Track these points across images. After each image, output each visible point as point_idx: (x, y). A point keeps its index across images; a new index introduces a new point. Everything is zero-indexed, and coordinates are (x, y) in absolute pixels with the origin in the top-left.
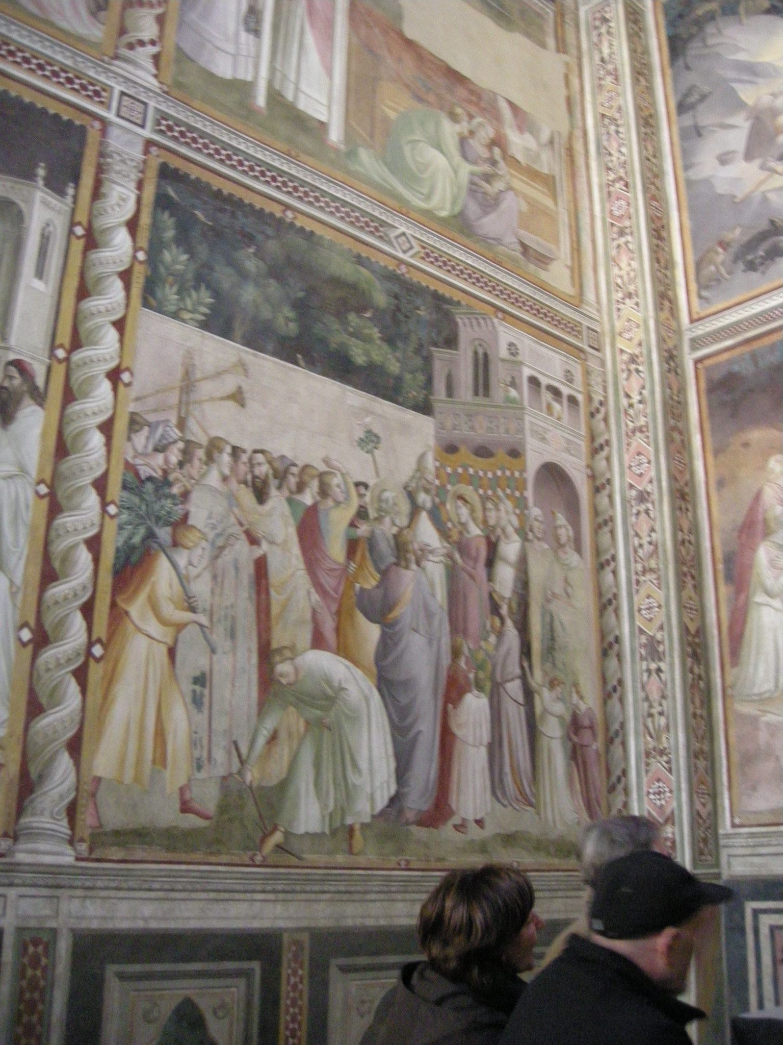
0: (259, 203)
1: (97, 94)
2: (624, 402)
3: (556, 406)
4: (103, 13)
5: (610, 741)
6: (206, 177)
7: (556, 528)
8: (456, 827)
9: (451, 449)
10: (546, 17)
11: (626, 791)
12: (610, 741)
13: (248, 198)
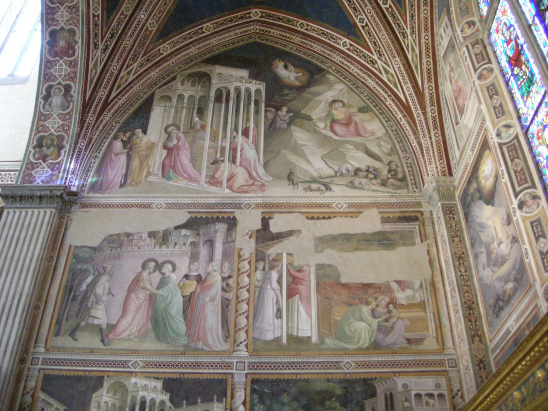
0: (286, 377)
1: (229, 366)
3: (431, 401)
4: (228, 339)
6: (266, 377)
10: (414, 230)
13: (282, 377)
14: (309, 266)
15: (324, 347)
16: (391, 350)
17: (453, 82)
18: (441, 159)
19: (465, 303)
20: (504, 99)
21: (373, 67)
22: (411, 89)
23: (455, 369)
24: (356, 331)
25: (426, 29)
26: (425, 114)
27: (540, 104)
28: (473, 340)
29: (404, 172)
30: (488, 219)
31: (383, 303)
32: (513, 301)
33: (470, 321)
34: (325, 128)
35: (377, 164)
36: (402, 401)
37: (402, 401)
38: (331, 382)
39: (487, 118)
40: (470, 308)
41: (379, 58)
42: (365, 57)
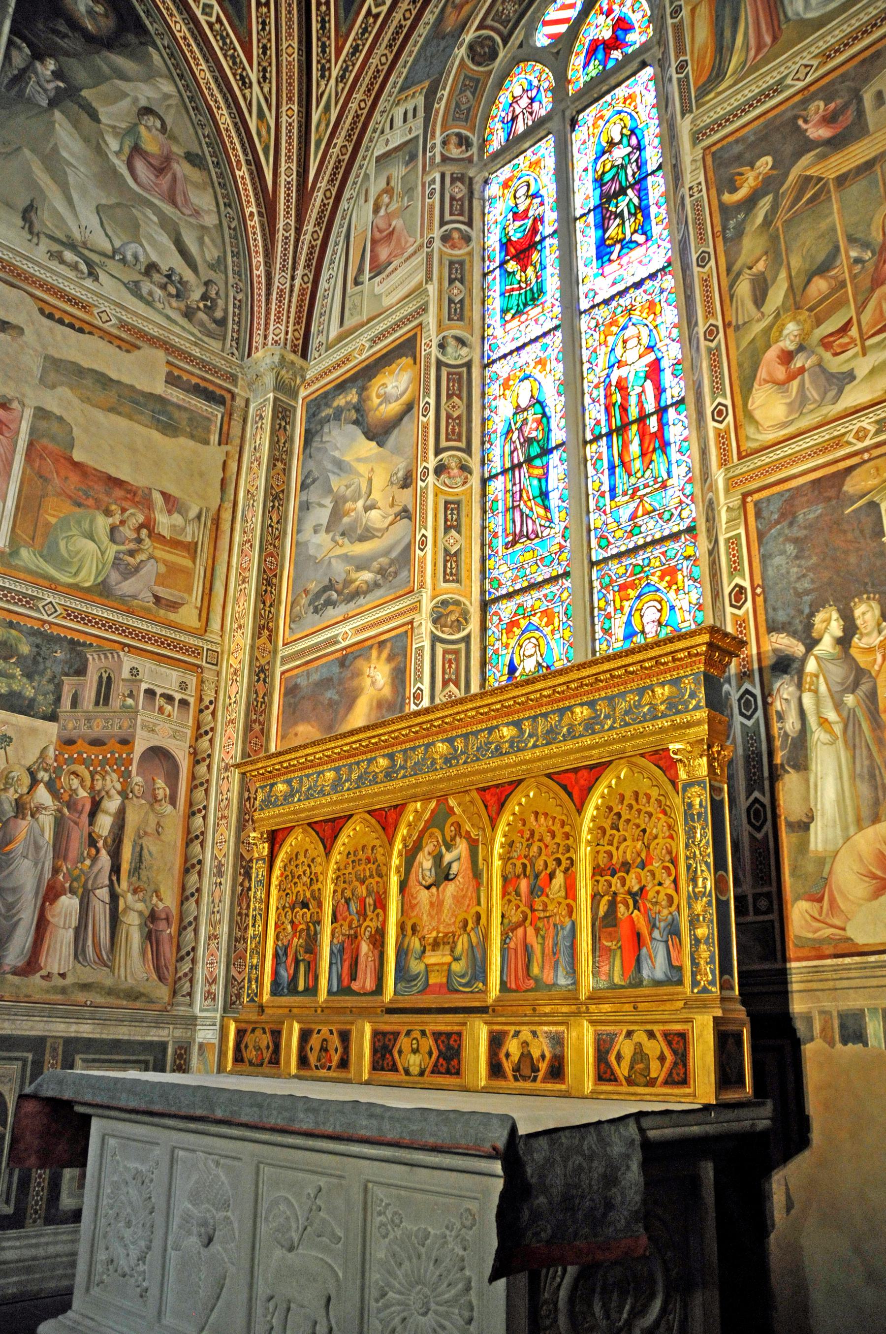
2: (228, 700)
3: (168, 708)
5: (182, 929)
7: (154, 790)
8: (42, 977)
9: (70, 742)
10: (213, 418)
11: (194, 961)
12: (182, 929)
14: (23, 405)
15: (16, 562)
16: (126, 605)
17: (382, 212)
18: (298, 323)
19: (265, 571)
20: (471, 295)
21: (241, 90)
22: (294, 176)
23: (214, 667)
24: (77, 553)
25: (369, 90)
26: (298, 230)
27: (536, 340)
28: (260, 633)
29: (226, 311)
30: (359, 460)
31: (133, 522)
32: (361, 600)
33: (264, 603)
34: (118, 154)
35: (188, 275)
36: (124, 695)
37: (124, 695)
38: (15, 629)
39: (433, 308)
40: (269, 583)
41: (259, 83)
42: (235, 63)
